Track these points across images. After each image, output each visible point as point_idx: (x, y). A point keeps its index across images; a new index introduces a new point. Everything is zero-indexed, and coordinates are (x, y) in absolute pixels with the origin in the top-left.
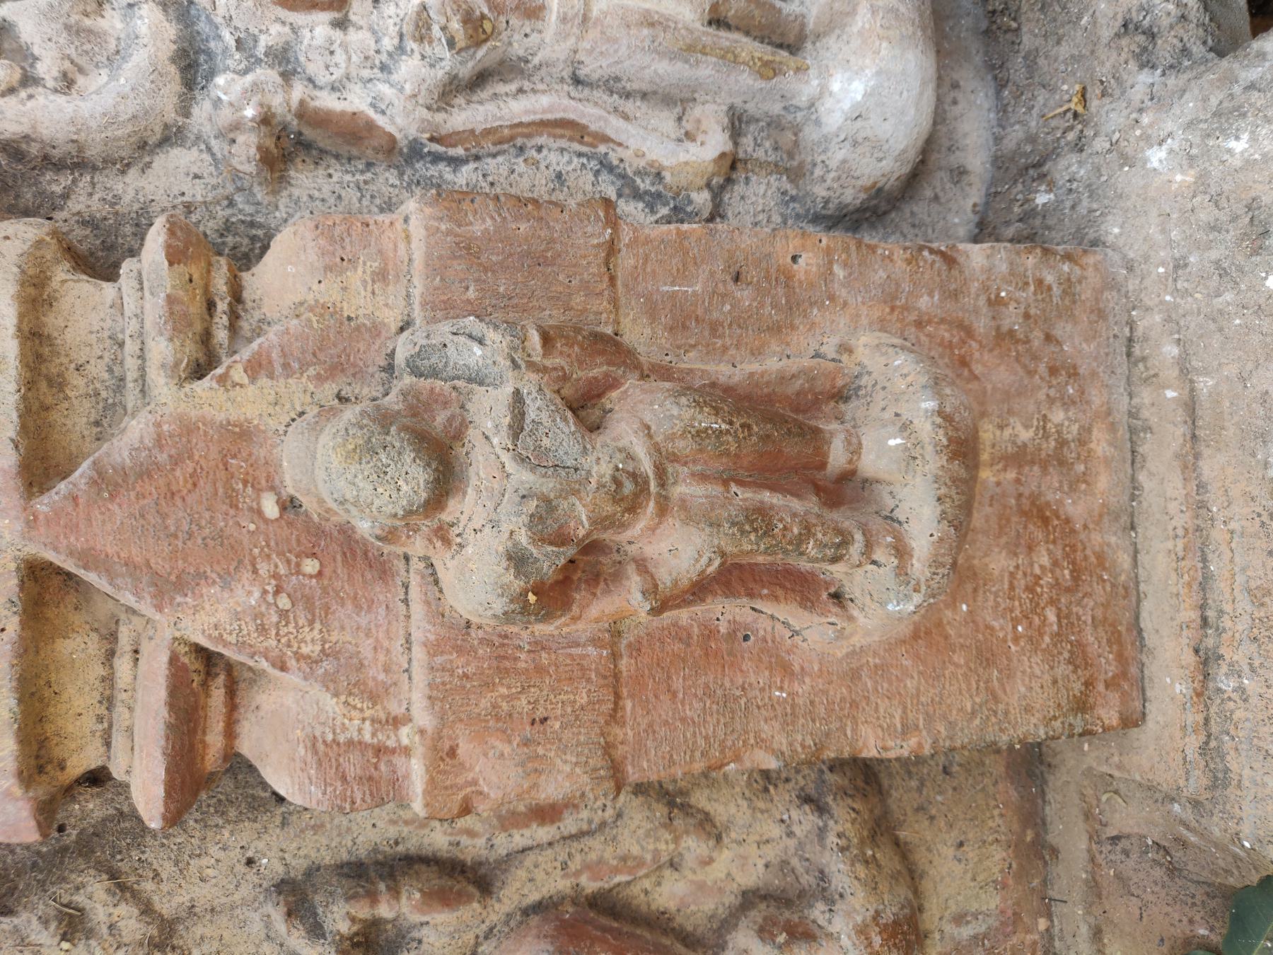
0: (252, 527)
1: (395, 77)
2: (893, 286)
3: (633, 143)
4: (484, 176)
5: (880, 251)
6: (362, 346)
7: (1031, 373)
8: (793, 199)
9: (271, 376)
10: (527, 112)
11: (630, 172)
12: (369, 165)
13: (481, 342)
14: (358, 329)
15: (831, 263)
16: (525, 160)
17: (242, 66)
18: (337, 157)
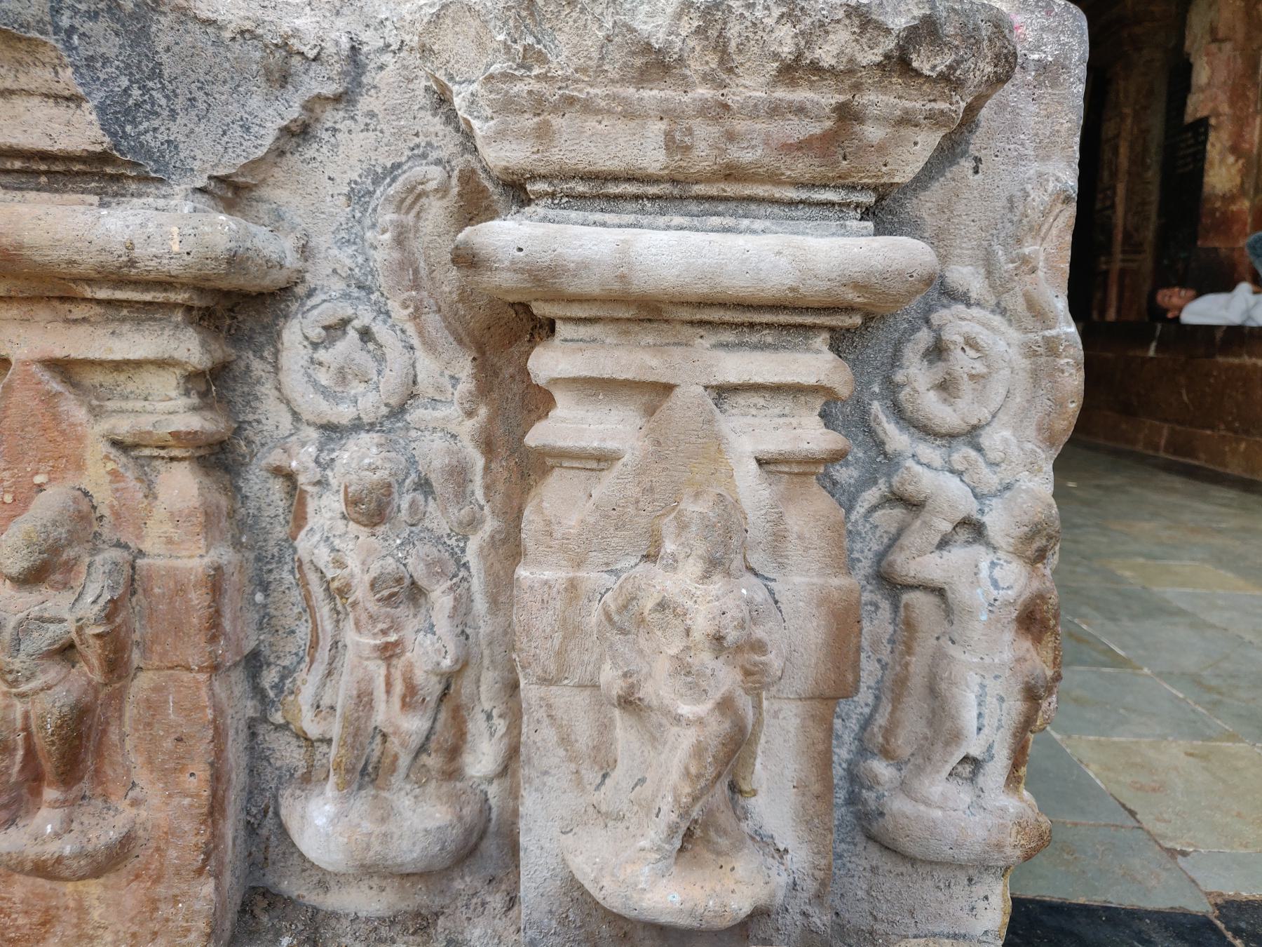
0: (29, 469)
1: (322, 544)
2: (181, 834)
3: (310, 678)
4: (288, 588)
5: (203, 827)
6: (131, 530)
7: (132, 920)
8: (292, 775)
9: (111, 482)
10: (321, 616)
11: (295, 675)
12: (288, 522)
13: (94, 602)
14: (140, 528)
15: (191, 796)
16: (300, 613)
17: (322, 460)
18: (291, 505)
